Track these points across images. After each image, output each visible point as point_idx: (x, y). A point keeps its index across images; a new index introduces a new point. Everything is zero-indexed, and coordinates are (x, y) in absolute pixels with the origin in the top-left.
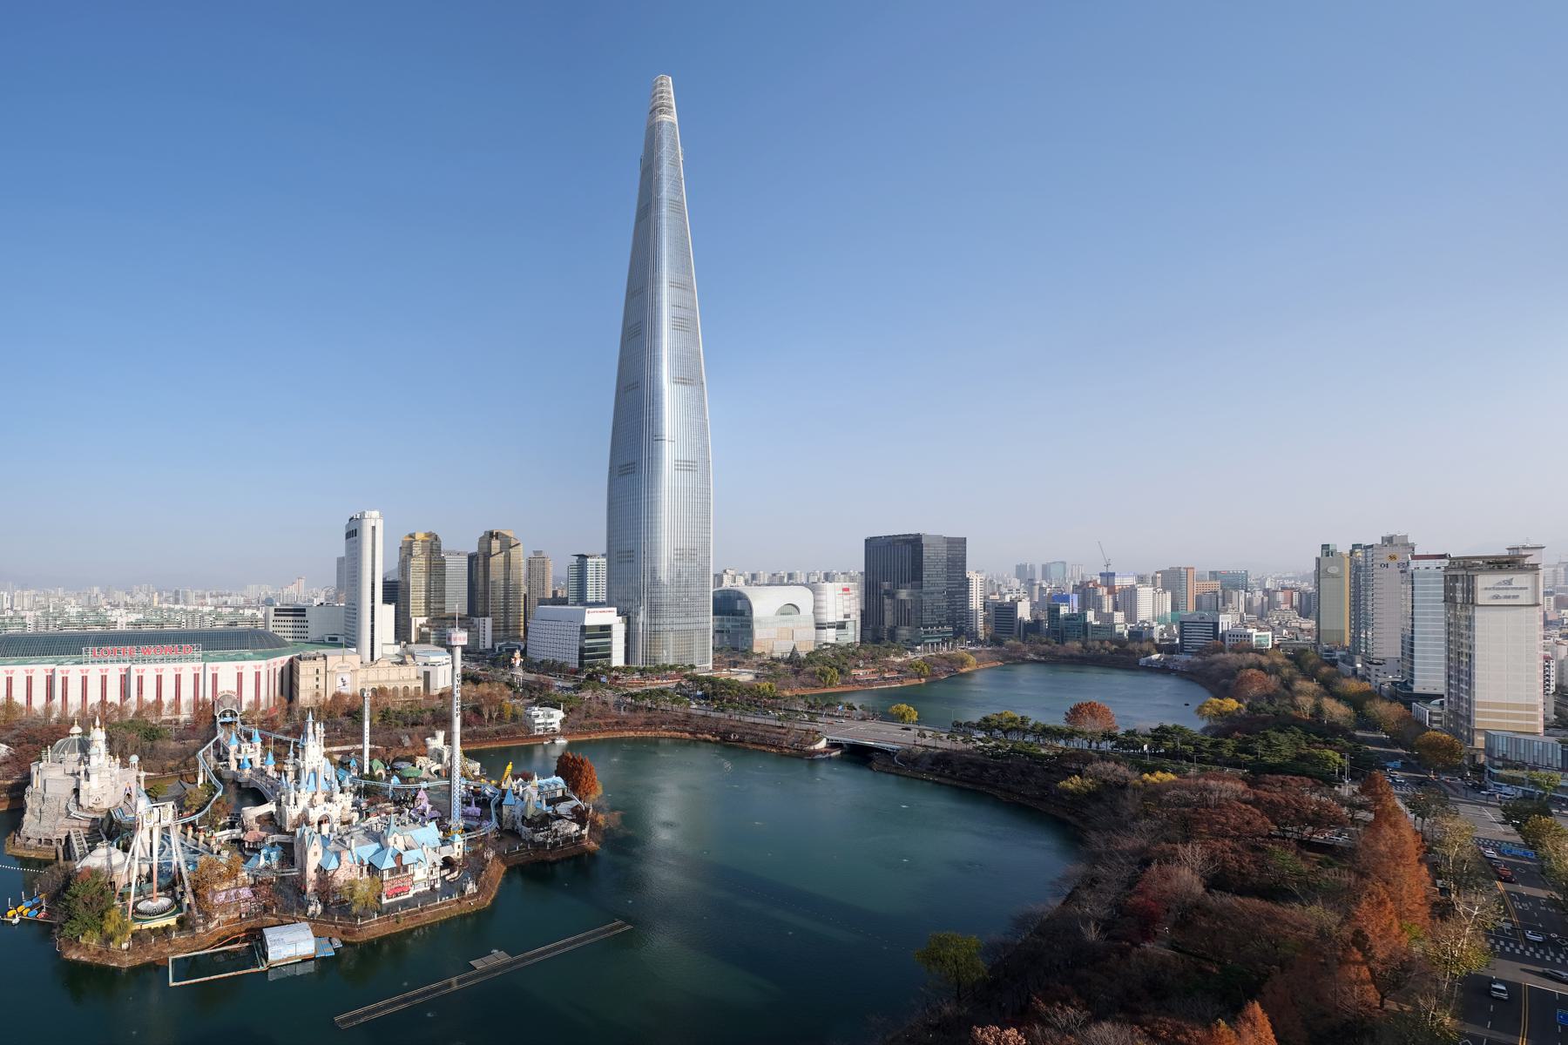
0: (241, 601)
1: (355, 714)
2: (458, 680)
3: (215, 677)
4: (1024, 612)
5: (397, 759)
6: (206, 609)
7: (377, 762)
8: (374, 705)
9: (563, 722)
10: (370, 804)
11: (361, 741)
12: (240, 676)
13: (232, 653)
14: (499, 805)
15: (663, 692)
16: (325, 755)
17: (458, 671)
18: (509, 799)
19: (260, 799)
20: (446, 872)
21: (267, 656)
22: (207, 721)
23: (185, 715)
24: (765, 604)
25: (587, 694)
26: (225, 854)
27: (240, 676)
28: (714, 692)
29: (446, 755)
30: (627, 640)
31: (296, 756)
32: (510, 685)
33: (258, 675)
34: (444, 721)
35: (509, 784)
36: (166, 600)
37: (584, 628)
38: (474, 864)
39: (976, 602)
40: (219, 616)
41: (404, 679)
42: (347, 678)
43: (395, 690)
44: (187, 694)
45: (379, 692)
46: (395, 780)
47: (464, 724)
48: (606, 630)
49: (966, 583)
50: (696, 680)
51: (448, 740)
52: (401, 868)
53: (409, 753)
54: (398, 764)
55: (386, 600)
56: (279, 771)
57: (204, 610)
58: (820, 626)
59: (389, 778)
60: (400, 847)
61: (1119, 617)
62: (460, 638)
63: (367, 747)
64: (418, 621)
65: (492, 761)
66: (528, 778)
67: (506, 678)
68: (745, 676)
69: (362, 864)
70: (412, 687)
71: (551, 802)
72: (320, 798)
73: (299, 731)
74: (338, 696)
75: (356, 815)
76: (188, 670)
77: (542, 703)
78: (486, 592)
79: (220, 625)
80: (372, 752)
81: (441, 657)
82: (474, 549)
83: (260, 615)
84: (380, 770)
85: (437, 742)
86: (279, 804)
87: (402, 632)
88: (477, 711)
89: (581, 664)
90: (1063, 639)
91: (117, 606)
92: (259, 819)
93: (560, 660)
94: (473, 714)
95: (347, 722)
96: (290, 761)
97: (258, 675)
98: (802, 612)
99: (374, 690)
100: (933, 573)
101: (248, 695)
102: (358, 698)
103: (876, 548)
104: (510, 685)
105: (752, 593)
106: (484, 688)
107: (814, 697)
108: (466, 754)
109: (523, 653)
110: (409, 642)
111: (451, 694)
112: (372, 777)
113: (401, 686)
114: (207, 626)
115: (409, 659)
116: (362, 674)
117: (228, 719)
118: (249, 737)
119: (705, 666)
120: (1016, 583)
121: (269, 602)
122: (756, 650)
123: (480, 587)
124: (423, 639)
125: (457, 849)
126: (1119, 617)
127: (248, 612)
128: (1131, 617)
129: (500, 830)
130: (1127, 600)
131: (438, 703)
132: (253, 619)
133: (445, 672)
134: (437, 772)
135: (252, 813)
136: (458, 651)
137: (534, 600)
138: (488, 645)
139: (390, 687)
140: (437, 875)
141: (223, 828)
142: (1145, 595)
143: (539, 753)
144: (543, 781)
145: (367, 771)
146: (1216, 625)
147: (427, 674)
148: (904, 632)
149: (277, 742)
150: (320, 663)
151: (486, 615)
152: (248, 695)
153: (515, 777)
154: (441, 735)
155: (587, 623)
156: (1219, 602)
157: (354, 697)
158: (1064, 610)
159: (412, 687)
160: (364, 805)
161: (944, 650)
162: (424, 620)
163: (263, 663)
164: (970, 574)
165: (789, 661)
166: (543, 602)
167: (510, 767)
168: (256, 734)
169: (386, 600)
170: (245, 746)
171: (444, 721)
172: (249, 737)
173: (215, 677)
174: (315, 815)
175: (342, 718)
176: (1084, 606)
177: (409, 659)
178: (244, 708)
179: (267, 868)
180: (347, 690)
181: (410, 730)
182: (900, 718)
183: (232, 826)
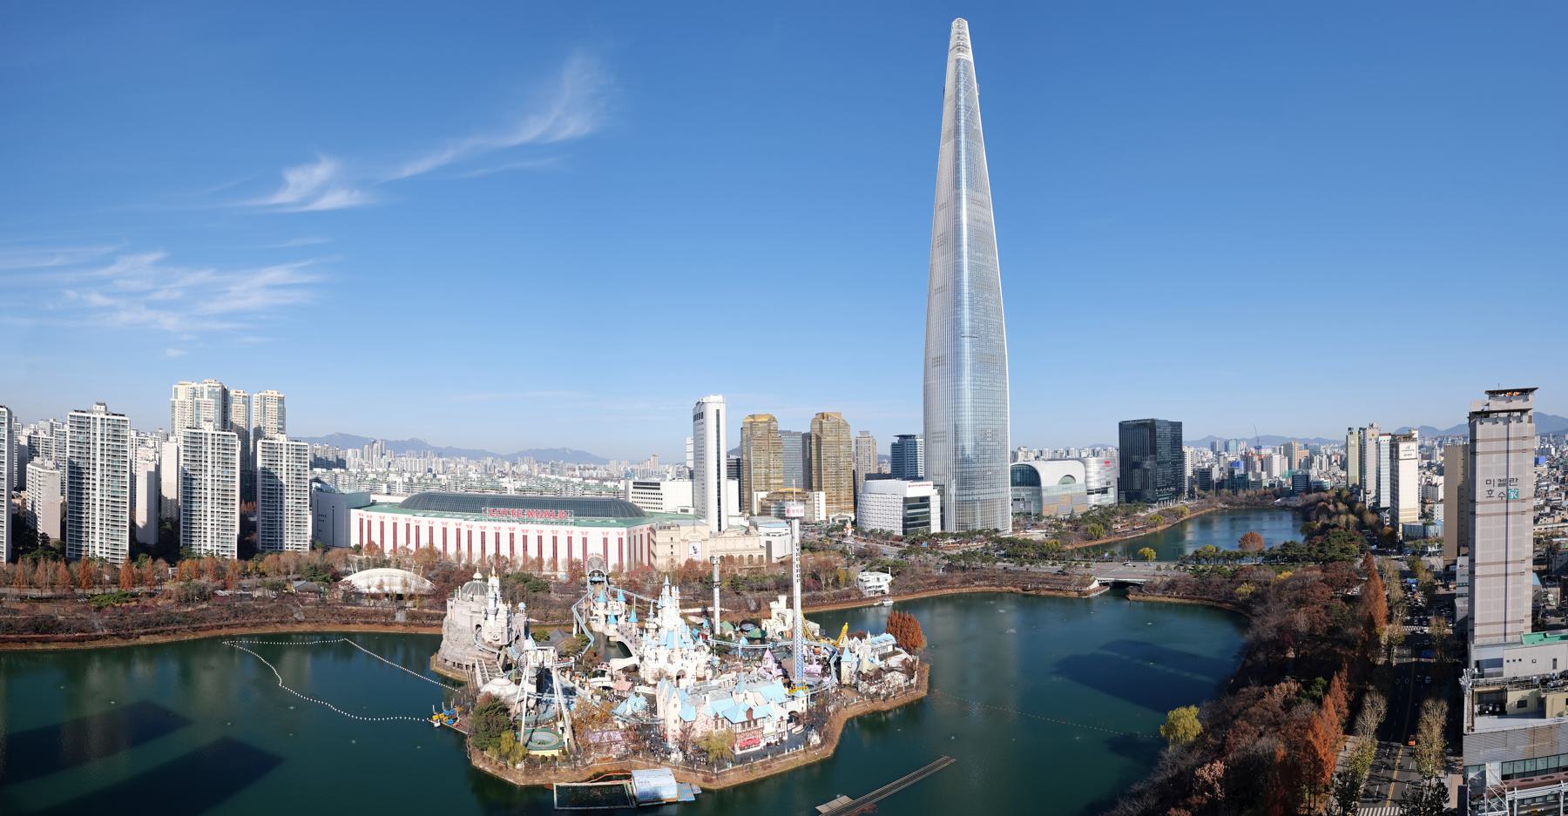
0: (605, 475)
1: (707, 582)
2: (796, 551)
3: (585, 540)
4: (1216, 475)
5: (744, 622)
6: (576, 480)
7: (727, 625)
8: (722, 572)
9: (892, 585)
10: (722, 662)
11: (712, 605)
12: (605, 540)
13: (598, 520)
14: (838, 664)
15: (974, 553)
16: (684, 616)
17: (797, 540)
18: (846, 657)
19: (627, 654)
20: (791, 725)
21: (626, 524)
22: (577, 581)
23: (562, 574)
24: (1050, 475)
25: (912, 557)
26: (597, 698)
27: (605, 540)
28: (1015, 550)
29: (784, 617)
30: (942, 509)
31: (656, 615)
32: (843, 553)
33: (620, 540)
34: (785, 586)
35: (845, 642)
36: (544, 470)
37: (906, 500)
38: (814, 719)
39: (1189, 472)
40: (587, 487)
41: (746, 547)
42: (698, 547)
43: (741, 557)
44: (562, 554)
45: (727, 560)
46: (743, 642)
47: (805, 589)
48: (924, 501)
49: (1182, 456)
50: (1000, 541)
51: (790, 604)
52: (751, 720)
53: (755, 616)
54: (745, 627)
55: (730, 477)
56: (642, 629)
57: (574, 483)
58: (1090, 492)
59: (739, 638)
60: (750, 703)
61: (1264, 475)
62: (795, 509)
63: (716, 609)
64: (759, 496)
65: (830, 623)
66: (862, 637)
67: (840, 547)
68: (1037, 535)
69: (716, 716)
70: (756, 556)
71: (883, 657)
72: (677, 654)
73: (657, 594)
74: (690, 563)
75: (710, 672)
76: (562, 532)
77: (870, 569)
78: (819, 469)
79: (589, 495)
80: (722, 614)
81: (781, 527)
82: (807, 430)
83: (621, 486)
84: (729, 631)
85: (778, 606)
86: (641, 659)
87: (744, 504)
88: (815, 577)
89: (905, 532)
90: (1235, 491)
91: (504, 475)
92: (625, 670)
93: (887, 529)
94: (813, 580)
95: (698, 587)
96: (651, 619)
97: (620, 540)
98: (1081, 477)
99: (722, 558)
100: (1164, 451)
101: (613, 559)
102: (708, 565)
103: (1124, 428)
104: (843, 553)
105: (1040, 466)
106: (822, 557)
107: (1087, 549)
108: (808, 617)
109: (854, 523)
110: (751, 514)
111: (791, 561)
112: (722, 637)
113: (746, 556)
114: (578, 495)
115: (752, 530)
116: (711, 543)
117: (596, 579)
118: (614, 595)
119: (1008, 532)
120: (1210, 455)
121: (628, 475)
122: (1045, 513)
123: (814, 464)
124: (765, 511)
125: (800, 706)
126: (1264, 475)
127: (610, 484)
128: (1270, 475)
129: (840, 685)
130: (1266, 464)
131: (782, 571)
132: (615, 491)
133: (783, 542)
134: (782, 634)
135: (618, 664)
136: (796, 523)
137: (861, 476)
138: (823, 518)
139: (736, 556)
140: (784, 727)
141: (595, 675)
142: (1276, 459)
143: (871, 614)
144: (875, 639)
145: (718, 632)
146: (1308, 477)
147: (769, 544)
148: (1148, 494)
149: (639, 601)
150: (672, 533)
151: (820, 489)
152: (613, 559)
153: (851, 637)
154: (783, 599)
155: (909, 495)
156: (1309, 462)
157: (705, 563)
158: (1237, 472)
159: (756, 556)
160: (717, 663)
161: (1171, 505)
162: (763, 495)
163: (624, 530)
164: (1185, 449)
165: (1068, 522)
166: (869, 477)
167: (846, 627)
168: (620, 592)
169: (730, 477)
170: (611, 603)
171: (785, 586)
172: (614, 595)
173: (585, 540)
174: (673, 671)
175: (694, 583)
176: (1247, 469)
177: (752, 530)
178: (610, 569)
179: (634, 715)
180: (697, 558)
181: (756, 595)
182: (1144, 558)
183: (603, 674)
